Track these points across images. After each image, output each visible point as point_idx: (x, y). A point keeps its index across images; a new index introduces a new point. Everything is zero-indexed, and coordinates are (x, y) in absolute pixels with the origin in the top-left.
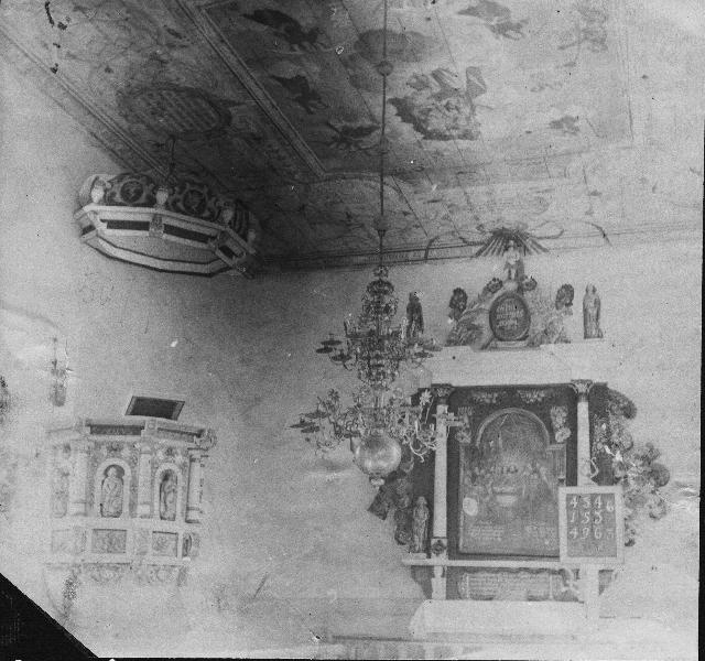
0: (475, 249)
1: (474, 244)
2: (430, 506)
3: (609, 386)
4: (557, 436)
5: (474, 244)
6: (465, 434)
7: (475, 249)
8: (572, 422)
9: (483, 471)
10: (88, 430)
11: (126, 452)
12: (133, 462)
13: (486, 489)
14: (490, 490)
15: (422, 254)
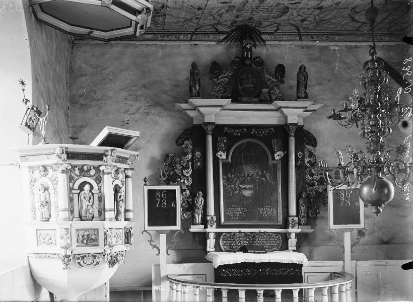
0: (223, 37)
1: (223, 33)
2: (205, 197)
3: (304, 128)
4: (275, 156)
5: (223, 33)
6: (222, 153)
7: (223, 37)
8: (286, 148)
9: (233, 176)
10: (65, 156)
11: (93, 172)
12: (99, 180)
13: (235, 187)
14: (237, 187)
15: (189, 37)
